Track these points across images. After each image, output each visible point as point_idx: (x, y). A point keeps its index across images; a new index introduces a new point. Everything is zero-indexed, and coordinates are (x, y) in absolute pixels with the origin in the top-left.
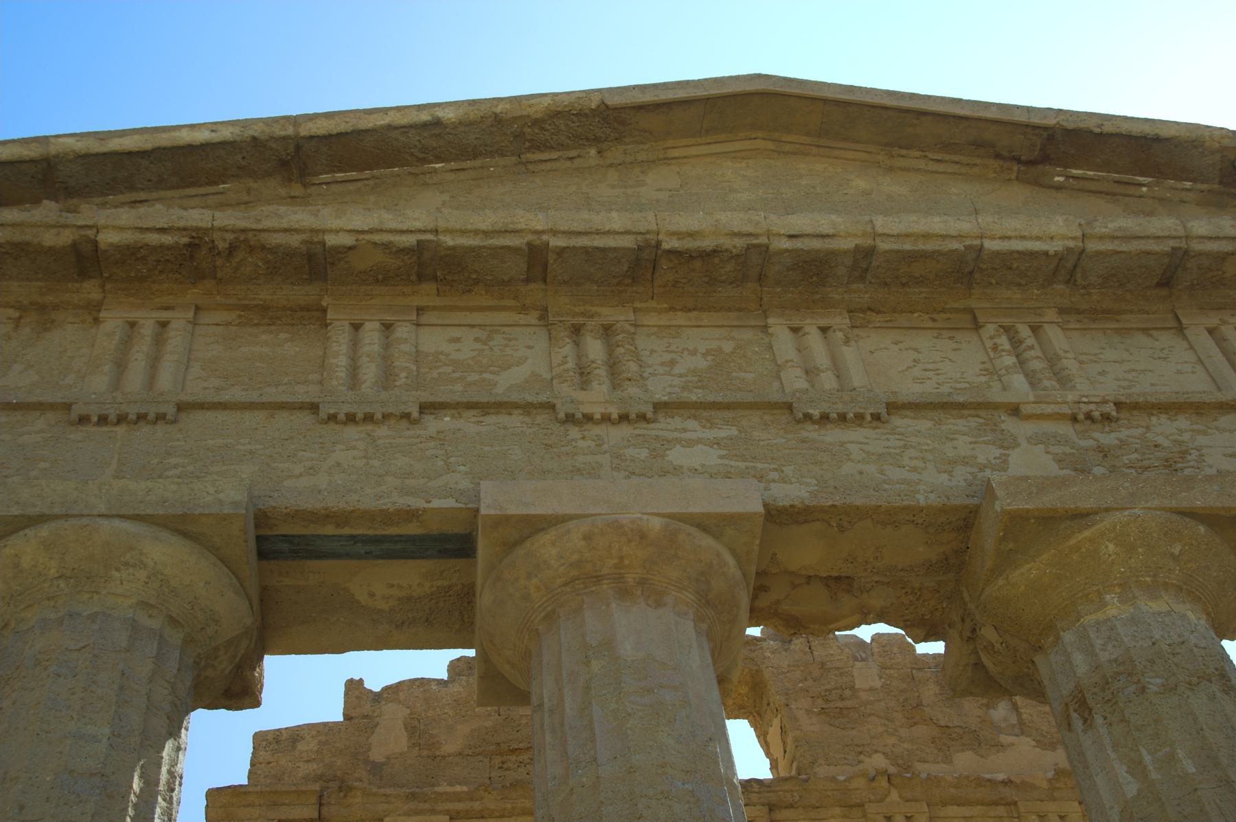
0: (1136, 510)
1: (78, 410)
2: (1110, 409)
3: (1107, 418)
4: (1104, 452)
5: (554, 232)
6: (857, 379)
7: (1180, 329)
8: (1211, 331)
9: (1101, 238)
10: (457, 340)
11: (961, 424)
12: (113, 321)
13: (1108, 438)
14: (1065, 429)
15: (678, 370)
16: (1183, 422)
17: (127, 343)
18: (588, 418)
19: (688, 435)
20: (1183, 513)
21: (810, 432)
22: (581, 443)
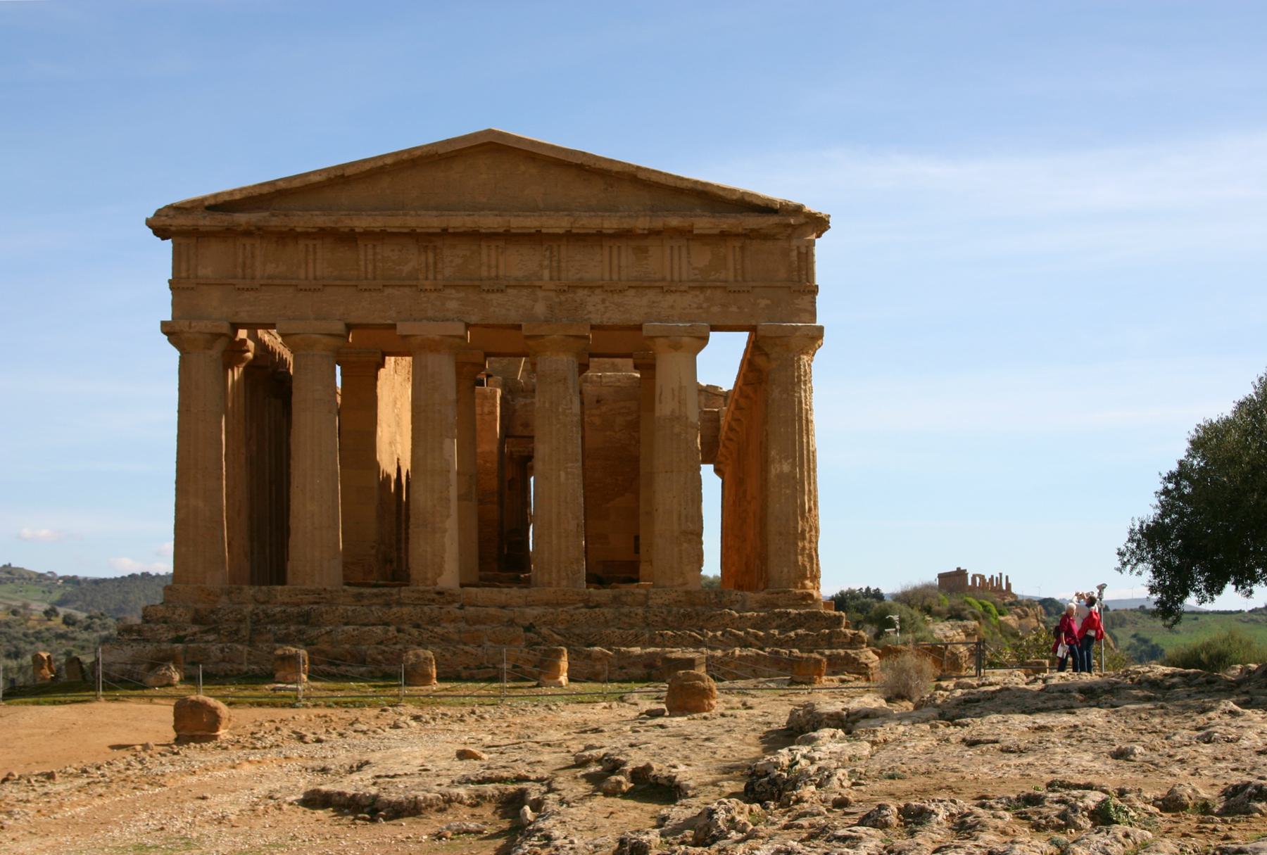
0: (555, 336)
1: (299, 287)
2: (566, 288)
3: (564, 291)
4: (560, 303)
5: (418, 227)
6: (501, 273)
7: (602, 246)
8: (611, 247)
9: (577, 228)
10: (393, 250)
11: (525, 292)
12: (302, 244)
13: (563, 298)
14: (553, 294)
15: (454, 265)
16: (586, 292)
17: (307, 251)
18: (426, 290)
19: (452, 296)
20: (567, 336)
21: (484, 295)
22: (425, 299)
